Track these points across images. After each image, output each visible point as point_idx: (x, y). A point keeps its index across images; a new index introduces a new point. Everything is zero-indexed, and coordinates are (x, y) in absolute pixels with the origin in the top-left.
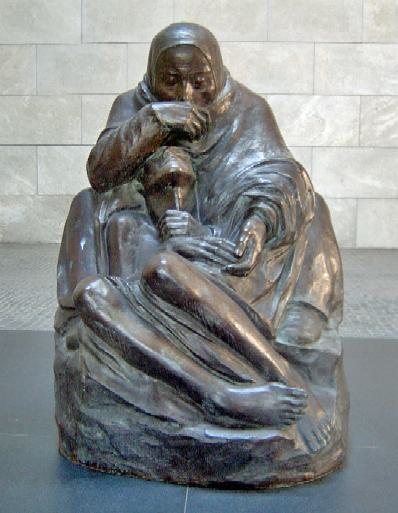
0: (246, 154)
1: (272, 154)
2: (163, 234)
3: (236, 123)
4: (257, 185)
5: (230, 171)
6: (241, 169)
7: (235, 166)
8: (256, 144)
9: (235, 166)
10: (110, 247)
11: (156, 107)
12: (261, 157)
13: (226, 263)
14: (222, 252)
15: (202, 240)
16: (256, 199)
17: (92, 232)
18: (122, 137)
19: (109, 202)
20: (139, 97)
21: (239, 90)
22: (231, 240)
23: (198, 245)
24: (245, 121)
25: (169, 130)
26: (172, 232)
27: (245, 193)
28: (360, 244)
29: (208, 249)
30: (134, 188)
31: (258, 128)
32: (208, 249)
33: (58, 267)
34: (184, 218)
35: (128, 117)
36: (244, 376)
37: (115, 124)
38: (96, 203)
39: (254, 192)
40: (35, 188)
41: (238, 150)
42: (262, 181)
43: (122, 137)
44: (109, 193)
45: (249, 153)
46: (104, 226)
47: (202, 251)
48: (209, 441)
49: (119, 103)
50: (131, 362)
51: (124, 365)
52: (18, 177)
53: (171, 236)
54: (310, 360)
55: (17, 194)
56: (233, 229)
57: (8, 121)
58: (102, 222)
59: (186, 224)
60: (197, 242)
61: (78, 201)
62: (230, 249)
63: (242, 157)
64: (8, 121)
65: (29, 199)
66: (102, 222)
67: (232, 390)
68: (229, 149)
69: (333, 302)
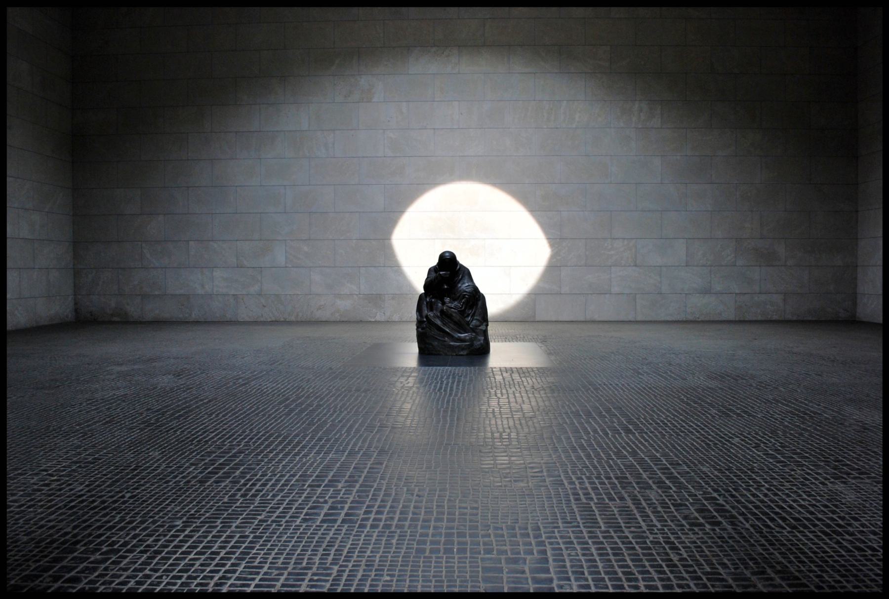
1: (470, 284)
2: (444, 303)
4: (466, 292)
8: (466, 281)
10: (431, 307)
11: (441, 273)
12: (467, 284)
16: (465, 295)
19: (429, 296)
21: (462, 266)
28: (538, 319)
31: (466, 277)
35: (433, 275)
38: (426, 297)
41: (461, 283)
45: (464, 283)
49: (430, 270)
50: (437, 330)
51: (436, 331)
54: (478, 331)
61: (421, 296)
63: (462, 284)
65: (355, 296)
67: (459, 335)
68: (459, 283)
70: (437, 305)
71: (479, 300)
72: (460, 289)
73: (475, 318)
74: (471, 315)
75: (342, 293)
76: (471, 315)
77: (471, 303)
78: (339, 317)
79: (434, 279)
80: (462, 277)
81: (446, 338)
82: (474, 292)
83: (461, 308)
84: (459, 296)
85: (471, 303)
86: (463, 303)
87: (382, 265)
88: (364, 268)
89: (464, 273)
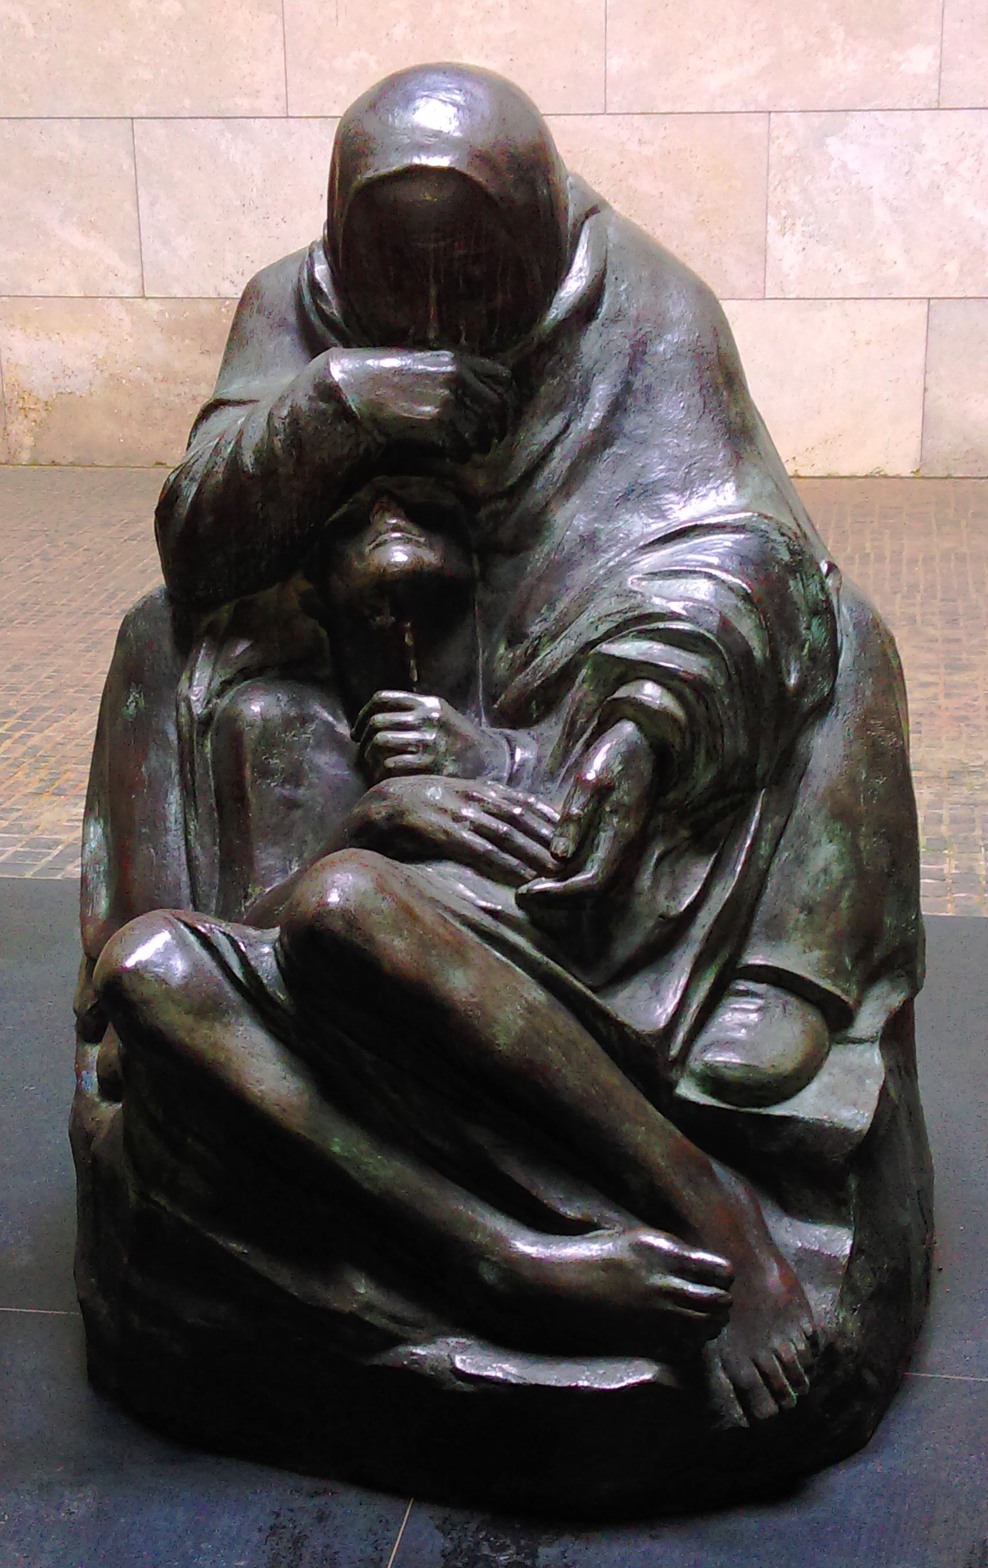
0: (626, 496)
3: (601, 392)
5: (569, 563)
6: (610, 558)
7: (590, 542)
9: (590, 542)
13: (528, 872)
14: (521, 839)
15: (468, 798)
17: (173, 737)
18: (248, 459)
19: (221, 640)
20: (307, 299)
22: (550, 803)
23: (458, 818)
24: (627, 387)
25: (381, 439)
26: (390, 762)
27: (606, 648)
29: (479, 830)
30: (294, 603)
32: (479, 830)
33: (86, 821)
34: (427, 722)
36: (571, 1212)
37: (234, 390)
39: (630, 648)
40: (134, 273)
42: (658, 604)
43: (248, 459)
44: (224, 613)
46: (210, 716)
47: (467, 835)
48: (468, 1388)
52: (76, 238)
53: (391, 773)
55: (75, 292)
56: (567, 752)
57: (30, 32)
58: (198, 710)
59: (430, 736)
60: (452, 804)
62: (546, 831)
64: (30, 32)
65: (115, 309)
66: (198, 710)
69: (877, 954)
70: (295, 776)
71: (824, 707)
72: (580, 576)
73: (755, 958)
74: (706, 918)
75: (37, 288)
76: (706, 918)
77: (704, 776)
78: (28, 441)
79: (265, 456)
80: (617, 407)
81: (363, 1288)
82: (747, 627)
83: (568, 866)
84: (567, 674)
85: (704, 776)
86: (602, 790)
87: (266, 105)
88: (158, 129)
89: (638, 352)
